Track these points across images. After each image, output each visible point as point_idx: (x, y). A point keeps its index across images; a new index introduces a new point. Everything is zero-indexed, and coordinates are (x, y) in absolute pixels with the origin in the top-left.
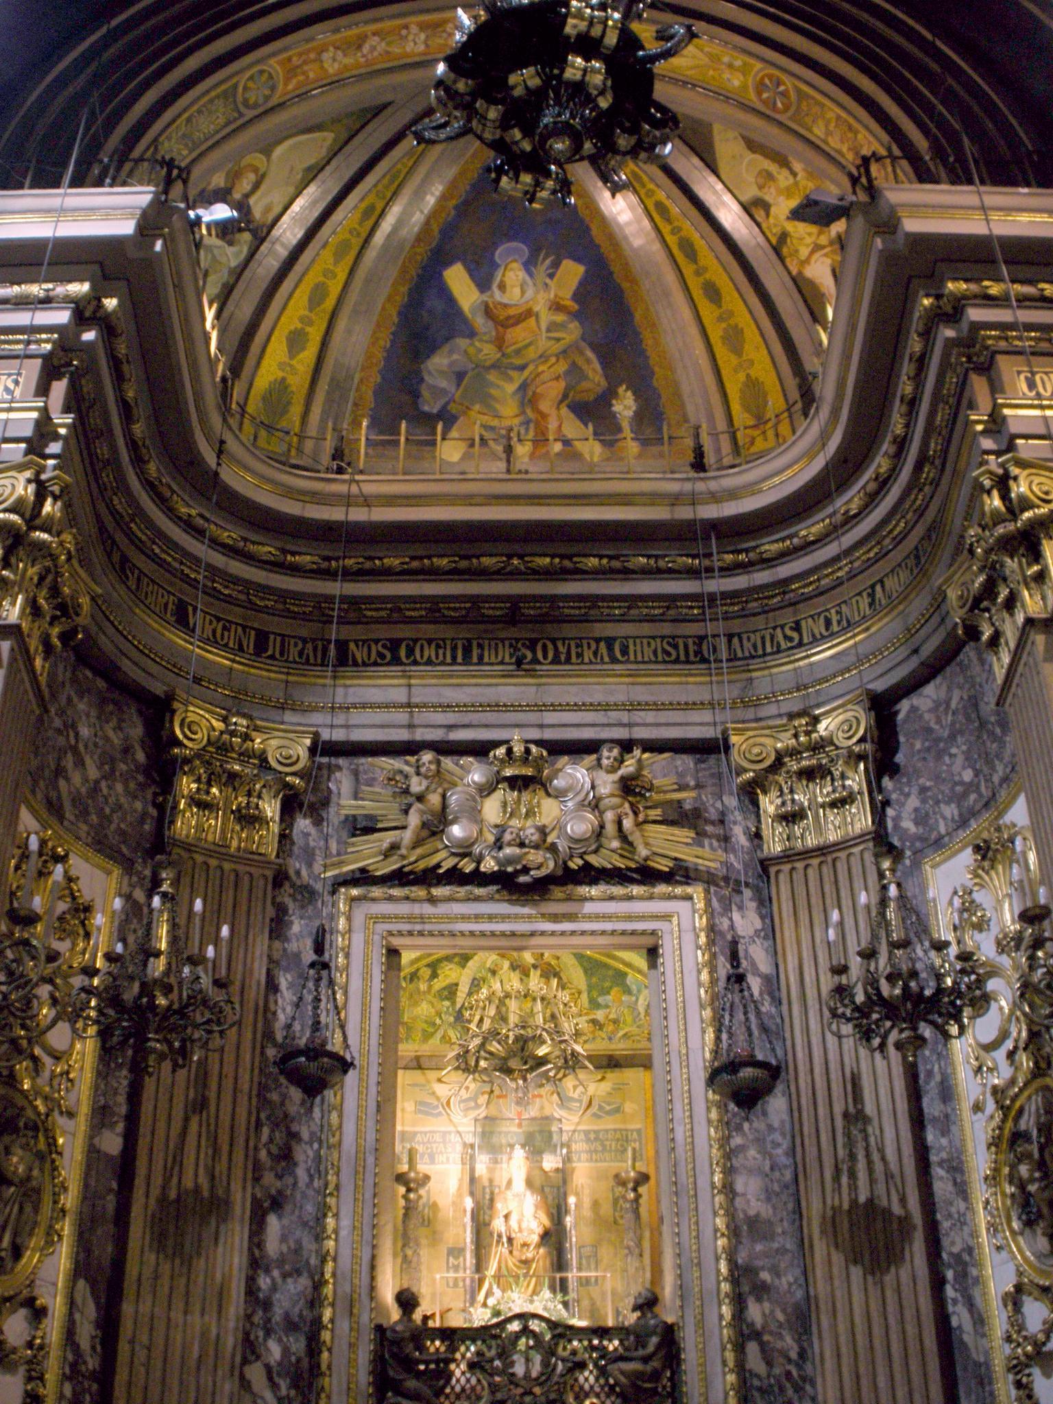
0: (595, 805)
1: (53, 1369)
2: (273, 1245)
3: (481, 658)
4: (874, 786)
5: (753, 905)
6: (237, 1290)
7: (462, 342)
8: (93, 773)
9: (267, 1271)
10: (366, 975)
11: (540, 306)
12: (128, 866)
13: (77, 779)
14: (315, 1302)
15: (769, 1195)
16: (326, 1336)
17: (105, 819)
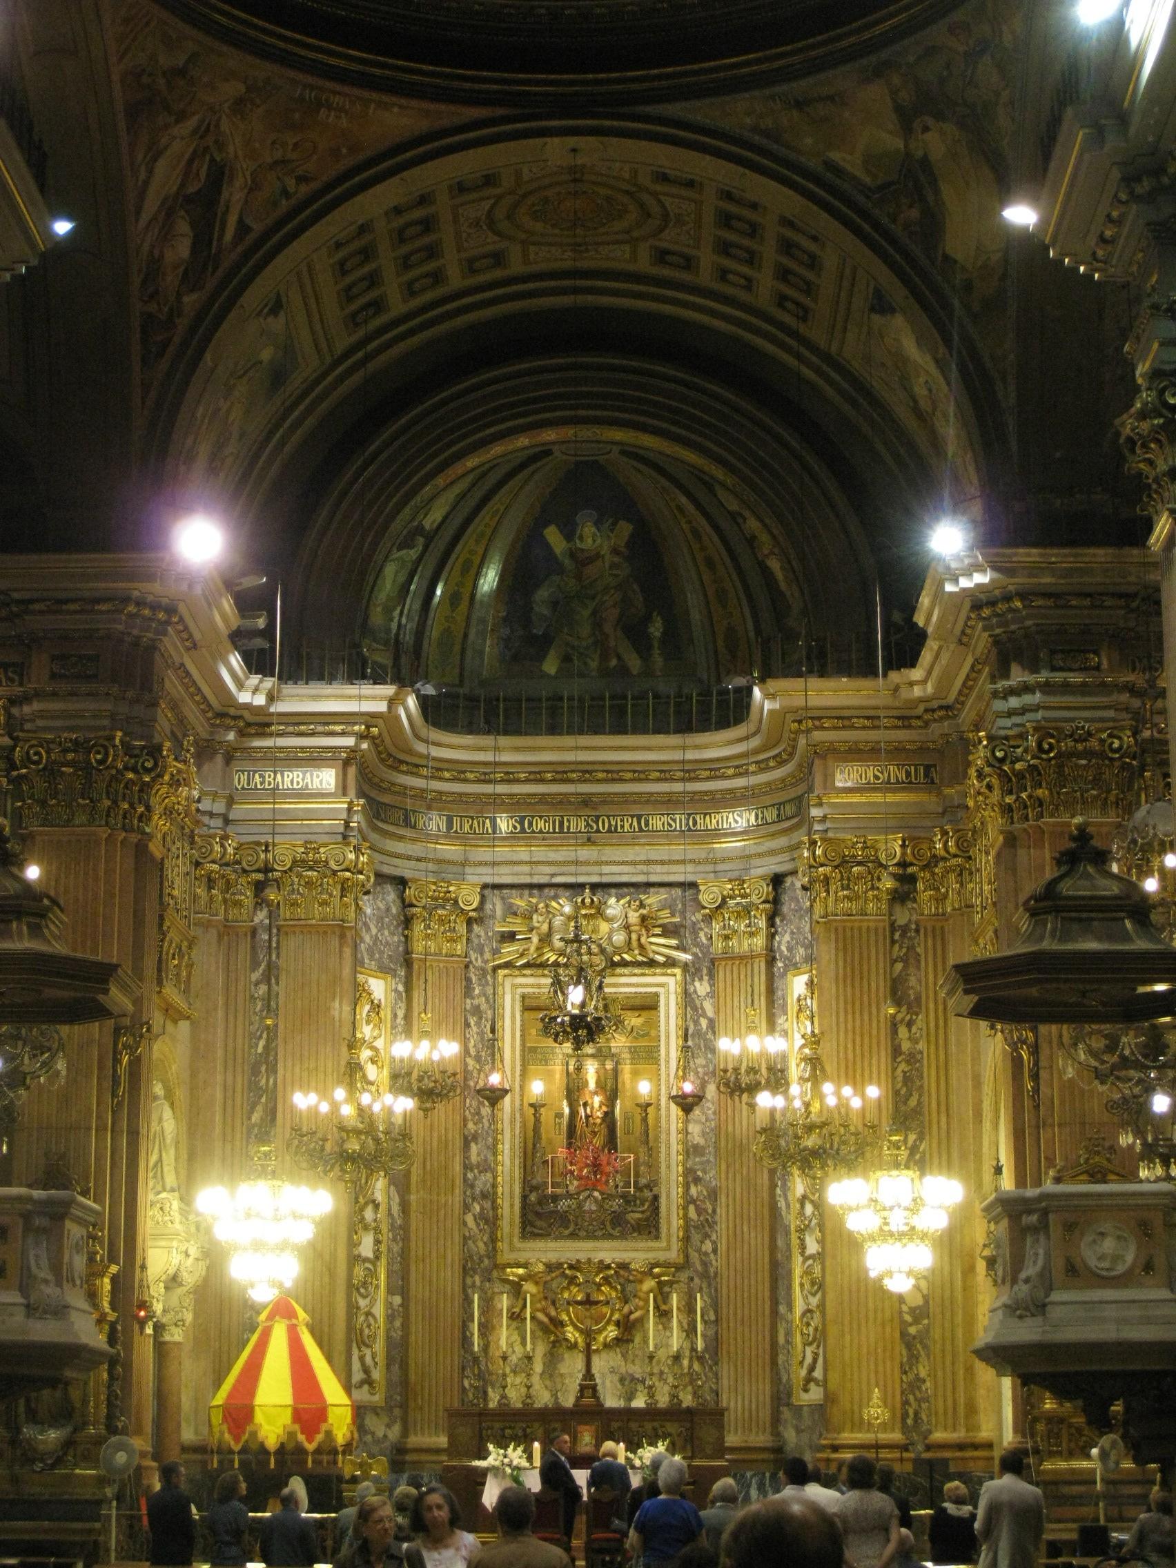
0: (627, 927)
2: (474, 1158)
3: (569, 828)
4: (771, 922)
5: (706, 978)
6: (458, 1181)
7: (556, 578)
8: (374, 931)
9: (472, 1170)
10: (513, 1022)
11: (605, 551)
12: (394, 976)
13: (367, 939)
14: (494, 1186)
15: (704, 1134)
16: (499, 1201)
17: (381, 952)
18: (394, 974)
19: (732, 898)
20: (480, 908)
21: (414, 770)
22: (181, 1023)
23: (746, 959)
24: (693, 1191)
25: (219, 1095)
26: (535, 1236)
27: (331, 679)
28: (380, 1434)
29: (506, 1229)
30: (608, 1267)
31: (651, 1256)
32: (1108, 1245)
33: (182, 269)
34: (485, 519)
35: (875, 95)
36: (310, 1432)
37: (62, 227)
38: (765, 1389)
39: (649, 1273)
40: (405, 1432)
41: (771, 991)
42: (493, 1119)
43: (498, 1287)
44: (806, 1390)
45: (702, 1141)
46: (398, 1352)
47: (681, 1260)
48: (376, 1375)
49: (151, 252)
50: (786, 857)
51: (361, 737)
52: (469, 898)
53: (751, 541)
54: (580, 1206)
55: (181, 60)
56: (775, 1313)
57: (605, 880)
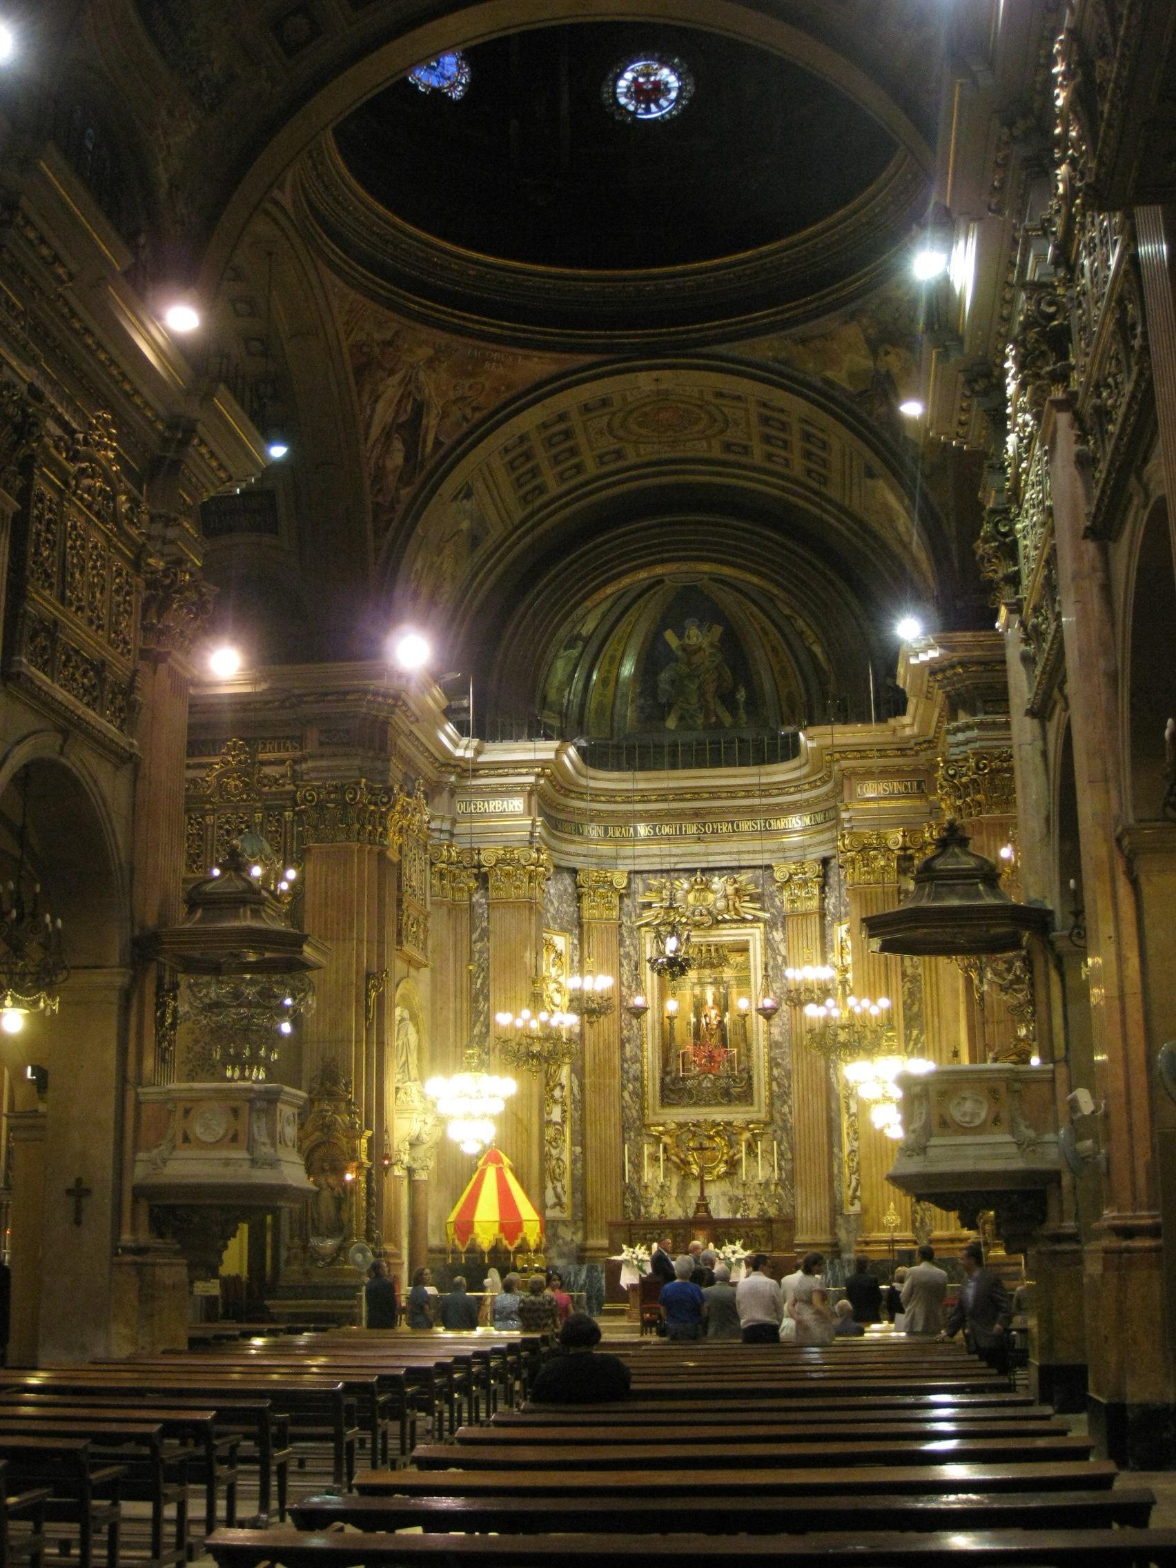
0: (726, 896)
1: (568, 1102)
2: (628, 1053)
8: (556, 904)
13: (552, 910)
14: (642, 1072)
15: (781, 1034)
18: (571, 932)
19: (796, 874)
20: (628, 886)
21: (580, 795)
22: (422, 970)
23: (805, 915)
24: (775, 1072)
25: (452, 1016)
26: (670, 1105)
27: (518, 738)
28: (568, 1238)
29: (651, 1101)
30: (719, 1124)
31: (748, 1117)
32: (969, 1106)
33: (398, 473)
34: (622, 627)
35: (852, 332)
36: (511, 1236)
37: (278, 452)
38: (826, 1202)
39: (746, 1128)
40: (585, 1238)
41: (823, 936)
42: (640, 1029)
43: (646, 1139)
44: (853, 1204)
45: (780, 1039)
46: (580, 1184)
47: (768, 1119)
48: (565, 1199)
49: (377, 463)
50: (830, 845)
51: (538, 776)
52: (620, 881)
53: (801, 634)
54: (700, 1084)
55: (388, 335)
56: (831, 1153)
57: (711, 865)
